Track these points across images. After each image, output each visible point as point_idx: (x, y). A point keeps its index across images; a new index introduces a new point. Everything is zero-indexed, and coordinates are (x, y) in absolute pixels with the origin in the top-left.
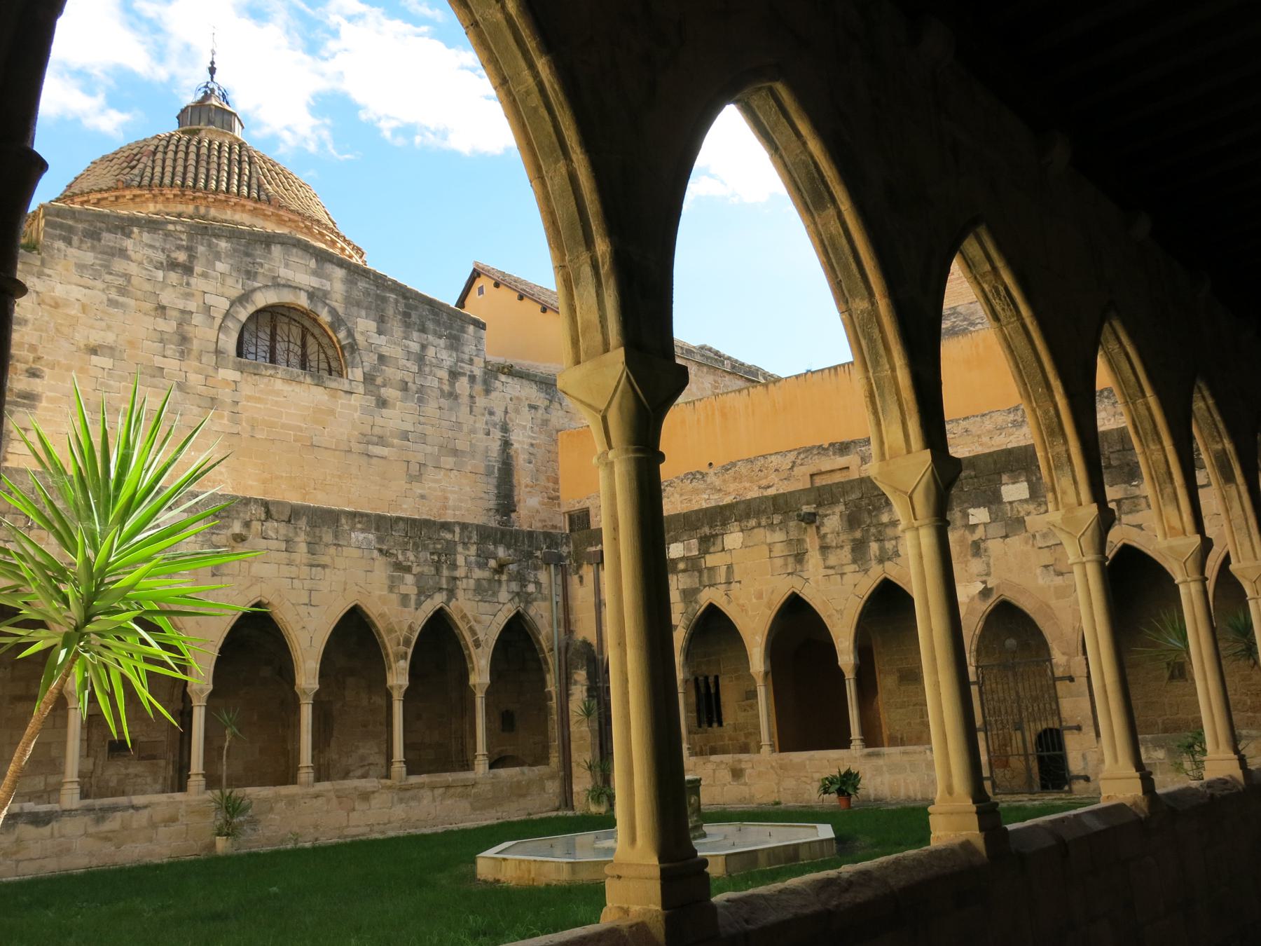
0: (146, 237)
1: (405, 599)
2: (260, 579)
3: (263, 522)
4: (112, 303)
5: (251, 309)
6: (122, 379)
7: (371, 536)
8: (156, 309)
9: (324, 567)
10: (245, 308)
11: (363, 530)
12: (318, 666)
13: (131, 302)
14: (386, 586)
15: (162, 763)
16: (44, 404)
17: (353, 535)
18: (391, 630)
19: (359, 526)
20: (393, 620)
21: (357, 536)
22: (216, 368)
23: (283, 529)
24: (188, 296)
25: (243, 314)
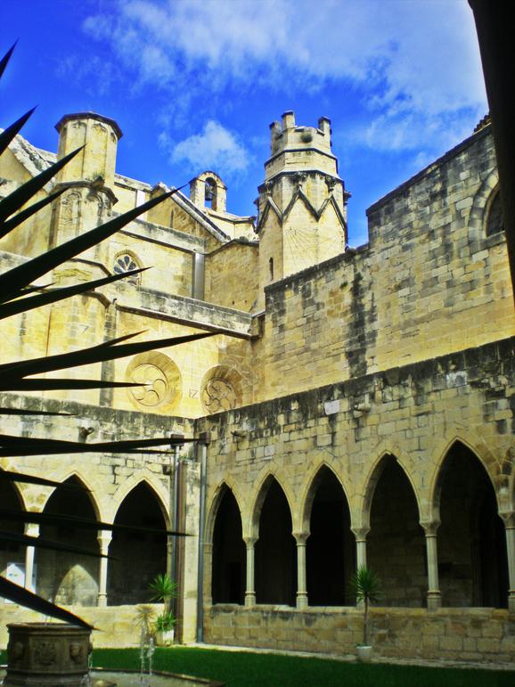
0: (417, 189)
1: (500, 425)
2: (382, 437)
3: (381, 389)
4: (405, 248)
5: (487, 193)
6: (415, 297)
7: (463, 374)
8: (429, 235)
9: (427, 413)
10: (482, 195)
11: (455, 370)
12: (431, 503)
13: (415, 240)
14: (482, 417)
15: (471, 582)
16: (379, 337)
17: (448, 377)
18: (491, 460)
19: (453, 367)
20: (490, 449)
21: (452, 377)
22: (471, 255)
23: (396, 391)
24: (445, 214)
25: (482, 203)
